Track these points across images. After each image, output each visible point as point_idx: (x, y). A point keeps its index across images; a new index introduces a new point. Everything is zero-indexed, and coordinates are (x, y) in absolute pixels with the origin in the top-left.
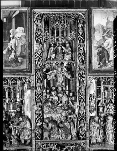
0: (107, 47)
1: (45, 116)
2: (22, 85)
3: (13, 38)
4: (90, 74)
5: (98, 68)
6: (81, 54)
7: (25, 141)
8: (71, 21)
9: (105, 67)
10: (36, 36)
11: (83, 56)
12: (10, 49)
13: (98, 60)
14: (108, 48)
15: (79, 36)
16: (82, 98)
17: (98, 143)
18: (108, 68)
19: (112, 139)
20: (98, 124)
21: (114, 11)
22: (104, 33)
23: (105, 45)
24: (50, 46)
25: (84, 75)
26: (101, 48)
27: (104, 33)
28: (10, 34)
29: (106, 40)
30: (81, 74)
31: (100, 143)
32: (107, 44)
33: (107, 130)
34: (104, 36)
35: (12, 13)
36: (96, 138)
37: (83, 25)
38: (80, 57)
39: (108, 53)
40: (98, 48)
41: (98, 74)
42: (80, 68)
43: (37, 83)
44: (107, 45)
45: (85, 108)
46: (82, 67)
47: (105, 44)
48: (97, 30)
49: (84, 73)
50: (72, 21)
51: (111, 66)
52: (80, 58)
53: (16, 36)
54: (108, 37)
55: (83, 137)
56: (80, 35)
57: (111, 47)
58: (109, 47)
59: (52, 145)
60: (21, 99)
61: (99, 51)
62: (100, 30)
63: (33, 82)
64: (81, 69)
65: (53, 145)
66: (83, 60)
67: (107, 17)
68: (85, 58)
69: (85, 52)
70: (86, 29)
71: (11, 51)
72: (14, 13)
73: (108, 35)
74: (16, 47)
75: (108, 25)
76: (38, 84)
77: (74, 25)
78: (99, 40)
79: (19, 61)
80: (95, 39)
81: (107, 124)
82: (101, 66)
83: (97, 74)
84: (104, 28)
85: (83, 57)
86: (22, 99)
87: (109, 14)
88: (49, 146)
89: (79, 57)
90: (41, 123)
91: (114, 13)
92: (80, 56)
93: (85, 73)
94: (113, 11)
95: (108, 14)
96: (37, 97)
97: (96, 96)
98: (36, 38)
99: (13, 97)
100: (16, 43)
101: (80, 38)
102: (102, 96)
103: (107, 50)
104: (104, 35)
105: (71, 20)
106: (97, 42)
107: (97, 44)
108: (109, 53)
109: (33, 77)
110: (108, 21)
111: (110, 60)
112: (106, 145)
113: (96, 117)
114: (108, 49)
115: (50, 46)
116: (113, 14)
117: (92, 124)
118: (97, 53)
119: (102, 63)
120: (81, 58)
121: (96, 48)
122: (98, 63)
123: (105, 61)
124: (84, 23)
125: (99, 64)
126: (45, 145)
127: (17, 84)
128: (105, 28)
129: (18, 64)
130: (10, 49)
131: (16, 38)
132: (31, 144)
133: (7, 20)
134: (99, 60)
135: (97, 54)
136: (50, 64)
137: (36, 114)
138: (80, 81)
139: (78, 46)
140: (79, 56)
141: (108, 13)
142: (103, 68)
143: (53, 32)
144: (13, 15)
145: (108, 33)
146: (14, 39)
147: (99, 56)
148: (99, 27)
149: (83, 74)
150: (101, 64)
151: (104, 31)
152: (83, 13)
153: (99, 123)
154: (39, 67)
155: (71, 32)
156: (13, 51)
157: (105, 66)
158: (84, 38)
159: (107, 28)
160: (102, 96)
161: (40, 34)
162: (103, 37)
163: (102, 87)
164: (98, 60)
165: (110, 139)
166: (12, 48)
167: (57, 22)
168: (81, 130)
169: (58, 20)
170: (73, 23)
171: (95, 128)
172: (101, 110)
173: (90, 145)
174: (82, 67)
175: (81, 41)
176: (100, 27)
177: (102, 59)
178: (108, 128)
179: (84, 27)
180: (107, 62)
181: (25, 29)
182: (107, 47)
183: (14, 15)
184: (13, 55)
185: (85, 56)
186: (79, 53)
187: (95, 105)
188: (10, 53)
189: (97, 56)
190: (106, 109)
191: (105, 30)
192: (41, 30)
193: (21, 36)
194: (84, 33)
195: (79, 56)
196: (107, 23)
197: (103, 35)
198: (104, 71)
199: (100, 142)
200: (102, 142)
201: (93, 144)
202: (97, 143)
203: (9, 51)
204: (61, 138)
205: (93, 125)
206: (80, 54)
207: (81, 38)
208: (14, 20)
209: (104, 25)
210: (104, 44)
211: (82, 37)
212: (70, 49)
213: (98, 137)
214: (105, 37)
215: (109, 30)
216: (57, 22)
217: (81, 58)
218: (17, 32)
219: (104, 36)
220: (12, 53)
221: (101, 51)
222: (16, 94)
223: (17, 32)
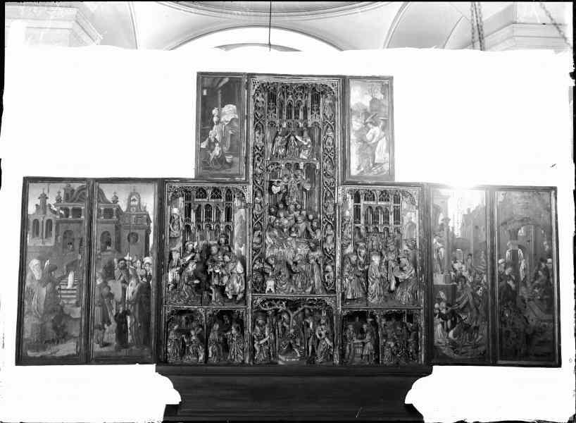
1: (268, 254)
2: (229, 198)
3: (218, 122)
7: (235, 296)
10: (255, 118)
12: (213, 140)
16: (329, 223)
23: (369, 136)
24: (277, 134)
28: (213, 116)
32: (371, 136)
34: (367, 123)
35: (217, 82)
43: (256, 196)
45: (334, 241)
46: (330, 171)
53: (222, 120)
55: (330, 288)
58: (374, 141)
59: (278, 302)
60: (227, 223)
63: (249, 199)
64: (328, 175)
65: (281, 303)
67: (371, 92)
69: (335, 147)
70: (338, 110)
71: (214, 144)
72: (220, 81)
73: (374, 122)
74: (223, 138)
76: (257, 199)
79: (228, 160)
86: (230, 224)
88: (274, 305)
90: (261, 266)
96: (255, 220)
97: (352, 218)
98: (254, 123)
99: (213, 218)
100: (222, 131)
102: (362, 221)
103: (373, 146)
104: (367, 121)
109: (250, 187)
111: (376, 162)
115: (277, 134)
124: (335, 99)
126: (267, 304)
127: (221, 198)
128: (369, 110)
129: (226, 166)
130: (213, 140)
131: (222, 122)
132: (244, 298)
133: (207, 92)
136: (278, 164)
137: (253, 249)
138: (326, 194)
143: (281, 112)
144: (218, 84)
145: (372, 118)
146: (220, 125)
154: (259, 171)
156: (217, 144)
159: (372, 111)
160: (362, 221)
161: (262, 116)
162: (366, 124)
163: (362, 205)
166: (215, 139)
167: (290, 96)
168: (328, 277)
169: (292, 94)
170: (316, 99)
181: (238, 108)
183: (221, 84)
184: (217, 151)
187: (350, 236)
188: (212, 147)
192: (263, 109)
193: (232, 120)
197: (365, 120)
203: (211, 146)
204: (295, 290)
208: (220, 91)
209: (367, 104)
212: (309, 140)
214: (369, 124)
215: (374, 113)
216: (290, 96)
218: (225, 114)
219: (367, 123)
220: (216, 148)
222: (218, 214)
223: (225, 114)
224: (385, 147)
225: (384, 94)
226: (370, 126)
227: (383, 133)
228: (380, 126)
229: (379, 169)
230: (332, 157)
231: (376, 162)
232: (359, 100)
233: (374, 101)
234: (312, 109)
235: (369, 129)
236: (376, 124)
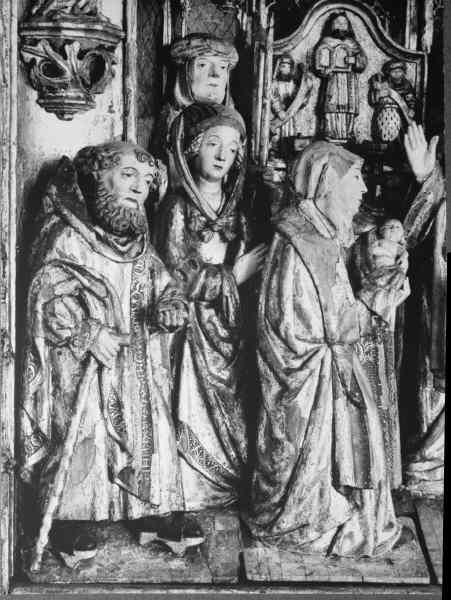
17: (148, 523)
19: (348, 477)
20: (150, 258)
31: (176, 525)
33: (278, 351)
36: (122, 461)
81: (279, 266)
112: (259, 551)
113: (114, 160)
117: (53, 255)
153: (162, 250)
165: (317, 468)
171: (97, 312)
172: (210, 79)
173: (30, 557)
178: (298, 310)
190: (280, 77)
199: (164, 510)
200: (214, 510)
201: (74, 534)
202: (131, 529)
205: (72, 268)
213: (151, 448)
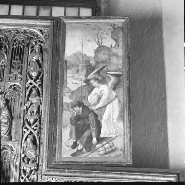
0: (95, 105)
4: (49, 171)
5: (73, 155)
6: (31, 123)
8: (13, 49)
9: (89, 153)
11: (35, 128)
13: (71, 138)
14: (97, 107)
15: (29, 82)
18: (97, 156)
21: (114, 25)
22: (88, 73)
23: (92, 98)
25: (33, 175)
26: (79, 107)
27: (88, 73)
29: (95, 87)
30: (28, 171)
32: (96, 97)
34: (89, 80)
37: (40, 58)
38: (28, 130)
39: (99, 118)
40: (73, 106)
41: (72, 172)
42: (25, 156)
44: (96, 101)
46: (31, 153)
47: (91, 100)
48: (73, 66)
49: (37, 170)
50: (16, 49)
51: (103, 152)
52: (27, 133)
54: (99, 83)
56: (32, 79)
57: (106, 106)
58: (100, 104)
61: (75, 115)
62: (80, 66)
64: (29, 160)
66: (34, 137)
67: (98, 37)
68: (38, 133)
69: (40, 118)
73: (100, 78)
75: (99, 56)
77: (20, 57)
78: (77, 89)
80: (68, 86)
82: (78, 151)
83: (66, 171)
84: (89, 61)
85: (35, 130)
87: (102, 31)
89: (26, 130)
91: (116, 30)
92: (28, 127)
93: (38, 169)
94: (111, 26)
95: (100, 32)
101: (32, 86)
103: (96, 112)
105: (13, 45)
106: (72, 93)
107: (71, 97)
108: (101, 118)
110: (100, 47)
111: (102, 135)
114: (97, 109)
116: (112, 32)
118: (71, 119)
119: (80, 142)
120: (31, 132)
121: (68, 107)
122: (71, 143)
123: (90, 138)
125: (75, 145)
128: (93, 63)
134: (74, 136)
135: (69, 120)
139: (26, 105)
140: (26, 128)
141: (100, 29)
142: (83, 156)
145: (98, 72)
147: (74, 127)
148: (78, 58)
149: (31, 171)
150: (80, 147)
151: (90, 68)
152: (41, 31)
155: (11, 72)
157: (88, 152)
158: (41, 85)
159: (98, 63)
162: (87, 81)
164: (71, 134)
174: (31, 153)
175: (34, 92)
176: (81, 59)
177: (83, 132)
179: (42, 60)
180: (94, 140)
182: (95, 105)
185: (40, 128)
186: (27, 120)
189: (70, 125)
191: (91, 65)
194: (41, 75)
195: (26, 128)
196: (97, 51)
197: (86, 76)
198: (86, 162)
206: (29, 123)
207: (35, 87)
210: (89, 97)
211: (37, 83)
214: (92, 81)
215: (101, 66)
217: (31, 133)
219: (89, 80)
221: (80, 113)
224: (116, 114)
225: (116, 40)
226: (95, 83)
227: (114, 94)
228: (110, 84)
229: (107, 146)
230: (35, 133)
231: (102, 135)
232: (79, 49)
233: (100, 49)
234: (11, 66)
235: (93, 88)
236: (103, 81)
